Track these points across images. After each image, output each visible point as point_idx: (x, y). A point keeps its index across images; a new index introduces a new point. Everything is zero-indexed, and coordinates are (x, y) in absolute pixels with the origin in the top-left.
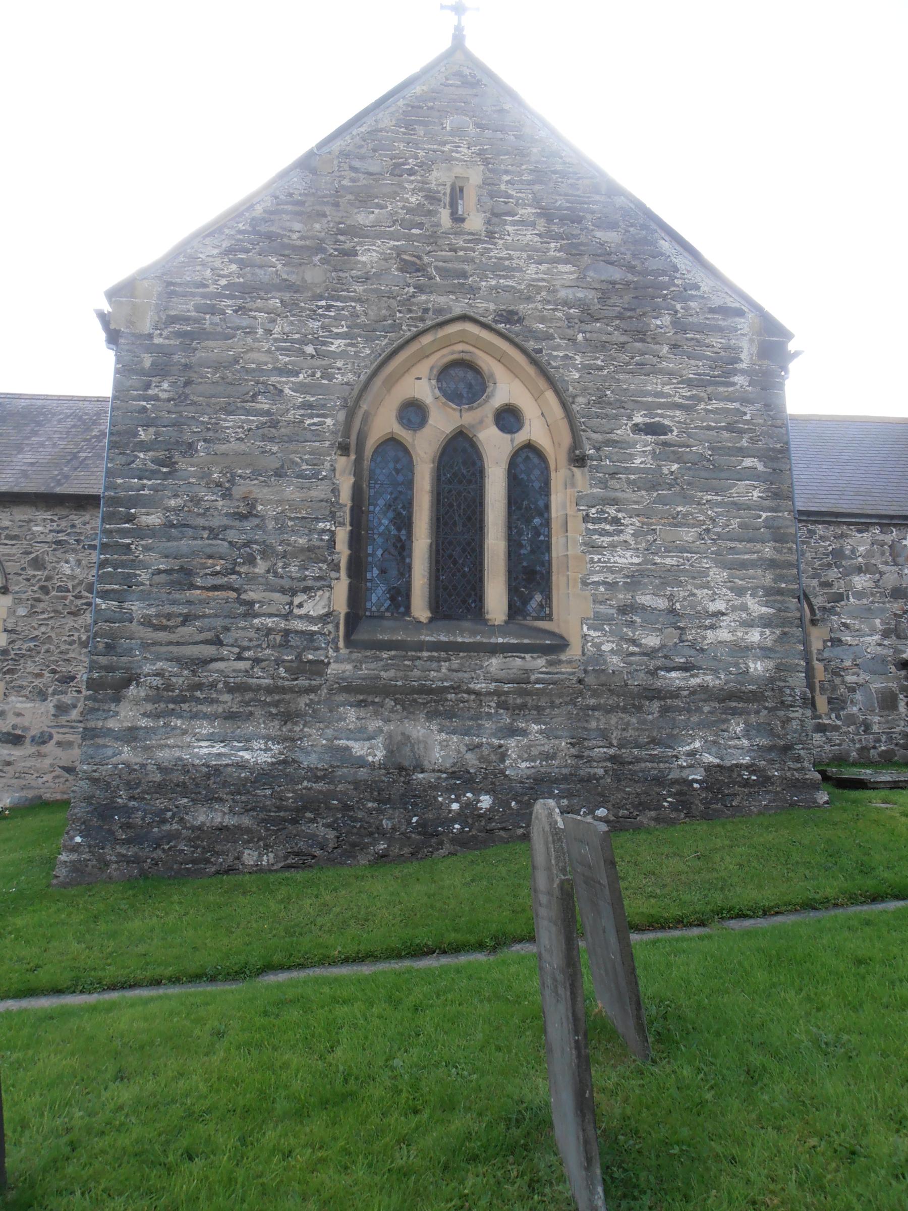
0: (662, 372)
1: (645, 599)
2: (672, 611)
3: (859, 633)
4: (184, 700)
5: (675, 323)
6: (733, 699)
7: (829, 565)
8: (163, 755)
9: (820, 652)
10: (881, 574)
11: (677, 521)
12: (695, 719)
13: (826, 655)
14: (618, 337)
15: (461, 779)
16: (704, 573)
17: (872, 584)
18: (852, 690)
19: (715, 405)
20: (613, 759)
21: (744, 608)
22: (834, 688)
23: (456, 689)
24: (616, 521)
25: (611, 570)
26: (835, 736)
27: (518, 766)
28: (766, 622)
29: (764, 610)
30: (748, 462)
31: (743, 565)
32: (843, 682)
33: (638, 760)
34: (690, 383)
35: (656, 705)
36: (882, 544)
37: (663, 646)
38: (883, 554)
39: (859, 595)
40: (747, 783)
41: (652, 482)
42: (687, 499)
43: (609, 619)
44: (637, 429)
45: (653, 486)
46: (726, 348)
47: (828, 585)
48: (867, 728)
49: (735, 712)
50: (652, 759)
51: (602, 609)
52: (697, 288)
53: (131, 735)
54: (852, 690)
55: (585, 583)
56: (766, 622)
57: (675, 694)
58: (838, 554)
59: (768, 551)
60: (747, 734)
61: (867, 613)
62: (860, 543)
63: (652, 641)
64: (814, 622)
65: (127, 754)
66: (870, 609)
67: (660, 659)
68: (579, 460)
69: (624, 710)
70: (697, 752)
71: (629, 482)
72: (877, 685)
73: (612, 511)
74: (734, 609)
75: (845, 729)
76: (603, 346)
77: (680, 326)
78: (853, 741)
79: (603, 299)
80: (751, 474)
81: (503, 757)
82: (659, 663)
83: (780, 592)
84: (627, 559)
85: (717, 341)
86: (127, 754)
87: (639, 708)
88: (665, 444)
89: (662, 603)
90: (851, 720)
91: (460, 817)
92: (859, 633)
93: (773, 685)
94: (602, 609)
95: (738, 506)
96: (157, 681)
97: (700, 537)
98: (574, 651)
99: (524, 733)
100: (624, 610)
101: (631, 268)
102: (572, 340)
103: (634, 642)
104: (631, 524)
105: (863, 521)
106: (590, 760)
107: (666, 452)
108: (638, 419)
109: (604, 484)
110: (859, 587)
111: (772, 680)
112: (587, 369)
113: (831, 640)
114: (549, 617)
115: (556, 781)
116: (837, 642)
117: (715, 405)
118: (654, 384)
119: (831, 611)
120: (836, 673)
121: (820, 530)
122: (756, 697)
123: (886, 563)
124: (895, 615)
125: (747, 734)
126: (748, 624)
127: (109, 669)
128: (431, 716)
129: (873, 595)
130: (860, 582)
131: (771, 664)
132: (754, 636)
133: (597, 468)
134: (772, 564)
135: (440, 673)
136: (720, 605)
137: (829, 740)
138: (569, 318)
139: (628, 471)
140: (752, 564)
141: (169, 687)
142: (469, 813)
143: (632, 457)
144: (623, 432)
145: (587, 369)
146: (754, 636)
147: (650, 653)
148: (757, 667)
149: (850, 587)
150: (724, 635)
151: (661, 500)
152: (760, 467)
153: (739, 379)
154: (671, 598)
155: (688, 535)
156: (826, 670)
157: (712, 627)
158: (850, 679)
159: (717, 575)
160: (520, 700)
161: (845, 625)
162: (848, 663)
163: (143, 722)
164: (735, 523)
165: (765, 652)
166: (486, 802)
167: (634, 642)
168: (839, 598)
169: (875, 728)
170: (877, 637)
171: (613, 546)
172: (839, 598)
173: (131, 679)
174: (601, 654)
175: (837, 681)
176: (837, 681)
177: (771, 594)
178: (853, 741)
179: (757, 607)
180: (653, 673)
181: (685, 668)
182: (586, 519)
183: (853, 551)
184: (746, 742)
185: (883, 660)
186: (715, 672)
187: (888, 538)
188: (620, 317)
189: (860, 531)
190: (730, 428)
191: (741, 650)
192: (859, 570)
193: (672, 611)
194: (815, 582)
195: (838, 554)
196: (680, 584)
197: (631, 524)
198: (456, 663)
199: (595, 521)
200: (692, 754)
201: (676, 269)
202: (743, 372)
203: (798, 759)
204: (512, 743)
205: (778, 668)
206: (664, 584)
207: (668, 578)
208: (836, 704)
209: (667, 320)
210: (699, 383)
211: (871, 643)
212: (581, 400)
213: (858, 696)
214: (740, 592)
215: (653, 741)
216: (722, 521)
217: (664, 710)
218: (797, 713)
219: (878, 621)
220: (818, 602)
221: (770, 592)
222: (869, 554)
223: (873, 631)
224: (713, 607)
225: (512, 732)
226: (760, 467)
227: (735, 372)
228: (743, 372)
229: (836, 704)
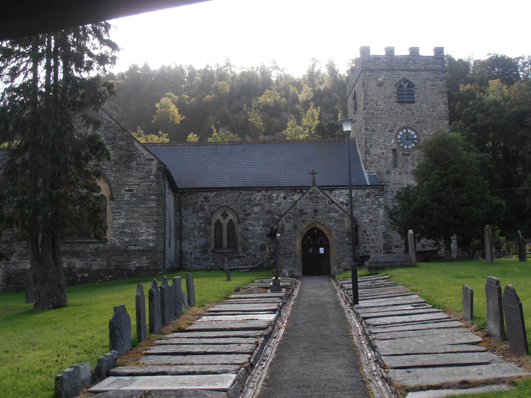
0: (133, 176)
1: (126, 230)
2: (132, 233)
3: (254, 226)
4: (24, 256)
5: (137, 164)
6: (143, 252)
7: (246, 204)
8: (21, 267)
9: (240, 233)
10: (264, 206)
11: (134, 212)
12: (135, 256)
13: (242, 234)
14: (123, 168)
15: (82, 270)
16: (140, 224)
17: (260, 210)
18: (251, 245)
19: (146, 183)
20: (116, 265)
21: (149, 231)
22: (245, 244)
23: (82, 252)
24: (120, 213)
25: (118, 224)
26: (244, 260)
27: (95, 267)
28: (154, 234)
29: (154, 231)
30: (152, 197)
31: (149, 221)
32: (248, 242)
33: (121, 266)
34: (139, 179)
35: (126, 254)
36: (265, 196)
37: (129, 241)
38: (265, 199)
39: (255, 214)
40: (145, 270)
41: (129, 203)
42: (137, 207)
43: (117, 235)
44: (126, 191)
45: (129, 204)
46: (149, 169)
47: (245, 211)
48: (255, 256)
49: (144, 255)
50: (125, 265)
51: (116, 233)
52: (143, 154)
53: (14, 263)
54: (251, 245)
55: (112, 227)
56: (154, 234)
57: (131, 251)
58: (249, 200)
59: (155, 218)
60: (146, 260)
61: (257, 219)
62: (258, 196)
63: (127, 240)
64: (239, 223)
65: (14, 267)
66: (259, 218)
67: (129, 243)
68: (112, 199)
69: (119, 255)
70: (135, 263)
71: (124, 203)
72: (260, 243)
73: (119, 210)
74: (147, 232)
75: (247, 257)
76: (119, 171)
77: (138, 164)
78: (250, 261)
79: (120, 158)
80: (153, 200)
81: (92, 266)
82: (128, 244)
83: (158, 227)
84: (122, 221)
85: (147, 168)
86: (14, 267)
87: (122, 255)
88: (132, 194)
89: (130, 231)
90: (249, 254)
91: (80, 278)
92: (254, 226)
93: (154, 248)
94: (116, 233)
95: (149, 208)
96: (19, 252)
97: (139, 215)
98: (109, 242)
99: (97, 260)
100: (121, 233)
101: (127, 150)
102: (112, 170)
103: (123, 240)
104: (124, 213)
105: (259, 189)
106: (111, 266)
107: (133, 196)
108: (127, 188)
109: (117, 204)
110: (256, 211)
111: (154, 247)
112: (115, 177)
113: (245, 229)
114: (105, 235)
115: (102, 270)
116: (246, 229)
117: (146, 183)
118: (131, 179)
119: (246, 219)
120: (246, 239)
121: (244, 192)
122: (149, 251)
123: (266, 202)
124: (268, 219)
125: (146, 260)
126: (150, 235)
127: (10, 250)
128: (77, 258)
129: (260, 213)
130: (256, 209)
131: (154, 244)
132: (151, 238)
133: (116, 201)
134: (156, 221)
135: (79, 248)
136: (143, 231)
137: (242, 261)
138: (111, 164)
139: (123, 201)
140: (151, 221)
141: (22, 253)
142: (83, 277)
143: (124, 197)
144: (123, 192)
145: (115, 177)
146: (151, 238)
147: (127, 242)
148: (151, 245)
149: (253, 211)
150: (144, 238)
151: (131, 207)
152: (155, 198)
153: (152, 177)
154: (132, 230)
155: (137, 215)
156: (242, 238)
157: (141, 236)
158: (250, 241)
159: (143, 224)
160: (96, 254)
161: (250, 224)
162: (250, 236)
163: (17, 261)
164: (148, 212)
165: (153, 241)
166: (86, 275)
167: (123, 240)
168: (248, 215)
169: (258, 257)
170: (260, 227)
171: (119, 218)
172: (248, 215)
173: (14, 251)
174: (115, 243)
175: (246, 242)
176: (246, 242)
177: (156, 228)
178: (250, 261)
179: (152, 231)
180: (127, 247)
181: (135, 245)
182: (113, 213)
183: (255, 199)
184: (146, 261)
185: (262, 235)
186: (141, 246)
187: (267, 194)
188: (124, 163)
189: (258, 192)
190: (149, 189)
191: (147, 241)
192: (256, 205)
193: (132, 233)
194: (240, 210)
195: (249, 200)
196: (134, 227)
197: (124, 213)
198: (83, 246)
199: (115, 213)
200: (134, 264)
201: (138, 150)
202: (153, 175)
203: (158, 265)
204: (94, 263)
205: (156, 245)
206: (130, 227)
207: (131, 225)
208: (245, 249)
209: (135, 163)
210: (142, 178)
211: (258, 229)
212: (113, 185)
213: (253, 247)
214: (148, 228)
215: (125, 262)
216: (145, 211)
217: (128, 255)
218: (159, 255)
219: (261, 222)
220: (241, 216)
221: (155, 227)
222: (260, 200)
223: (259, 225)
224: (141, 231)
225: (94, 260)
226: (155, 198)
227: (151, 175)
228: (153, 175)
229: (245, 249)
